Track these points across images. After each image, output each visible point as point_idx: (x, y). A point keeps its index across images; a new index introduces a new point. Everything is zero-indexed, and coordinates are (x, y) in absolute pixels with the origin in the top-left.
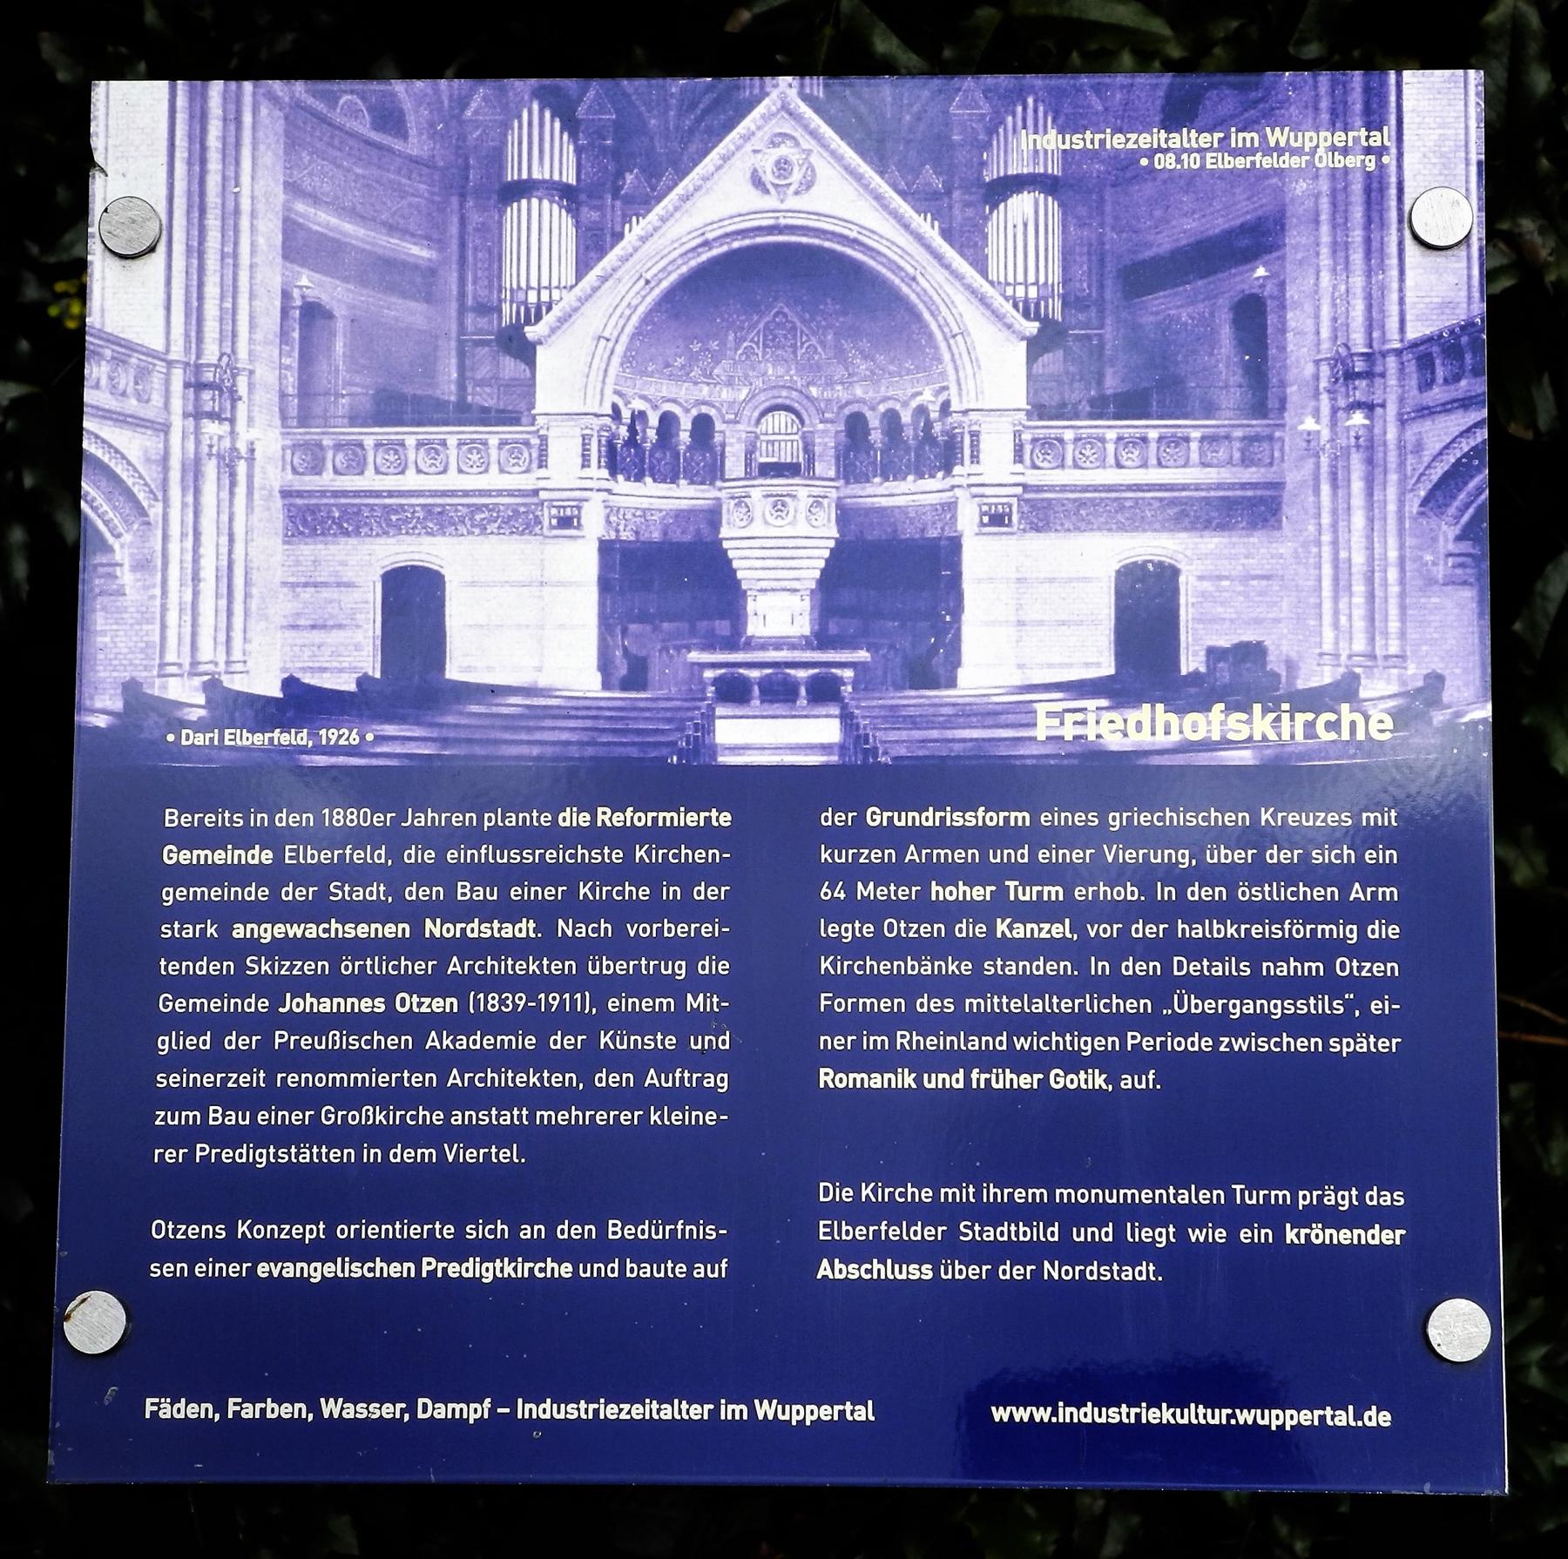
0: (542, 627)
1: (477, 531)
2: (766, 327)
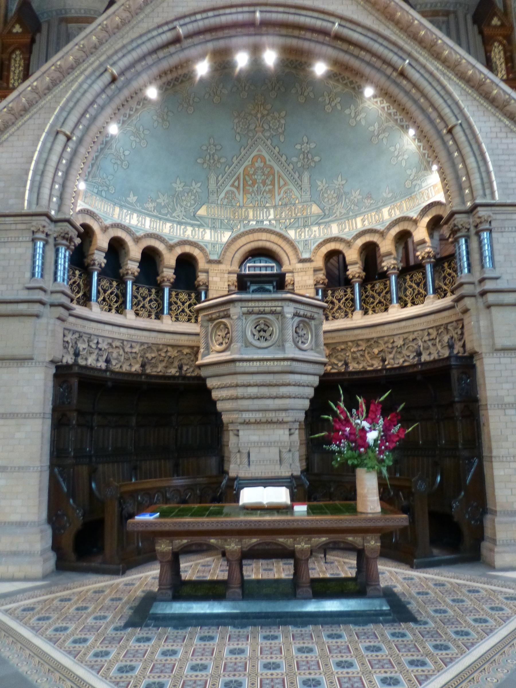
2: (246, 173)
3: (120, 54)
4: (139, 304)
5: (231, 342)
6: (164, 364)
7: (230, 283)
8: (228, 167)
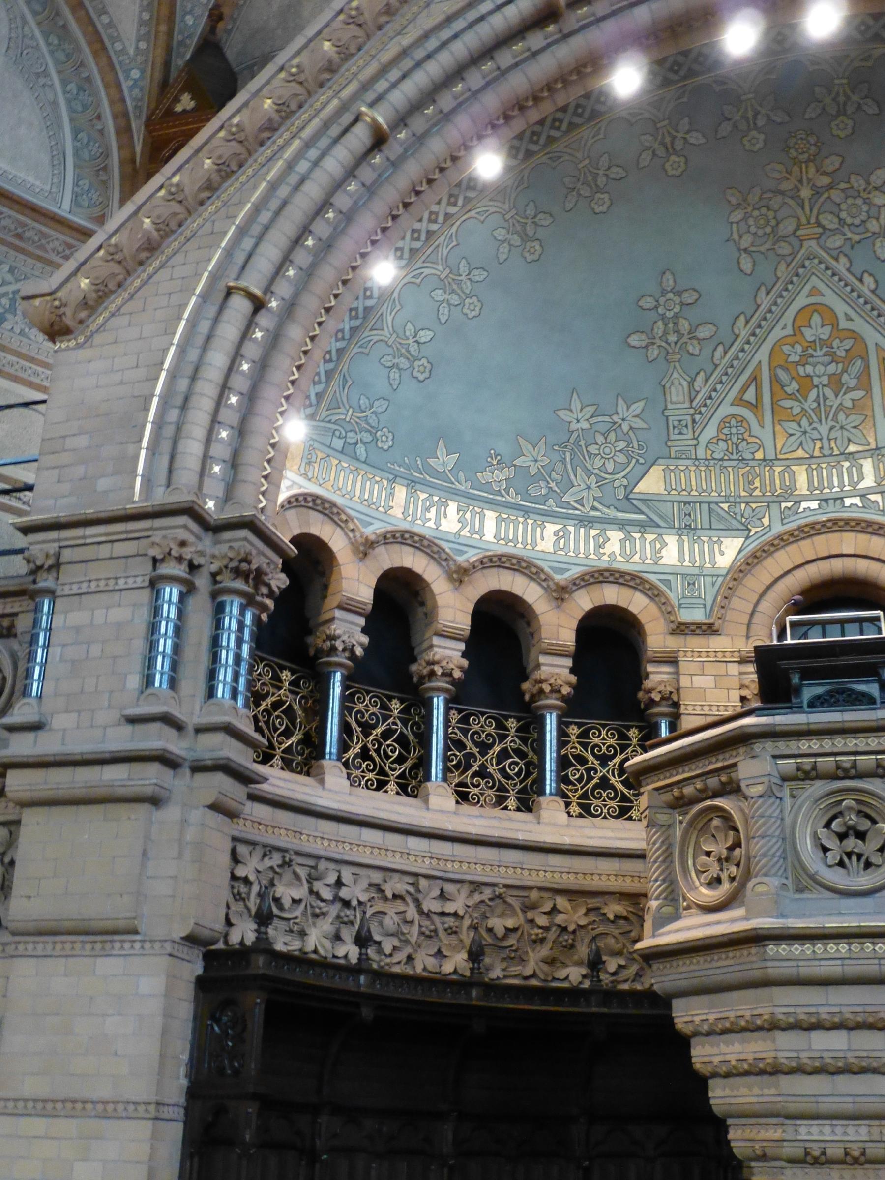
3: (394, 74)
4: (468, 766)
5: (747, 875)
6: (544, 951)
7: (745, 693)
8: (720, 349)
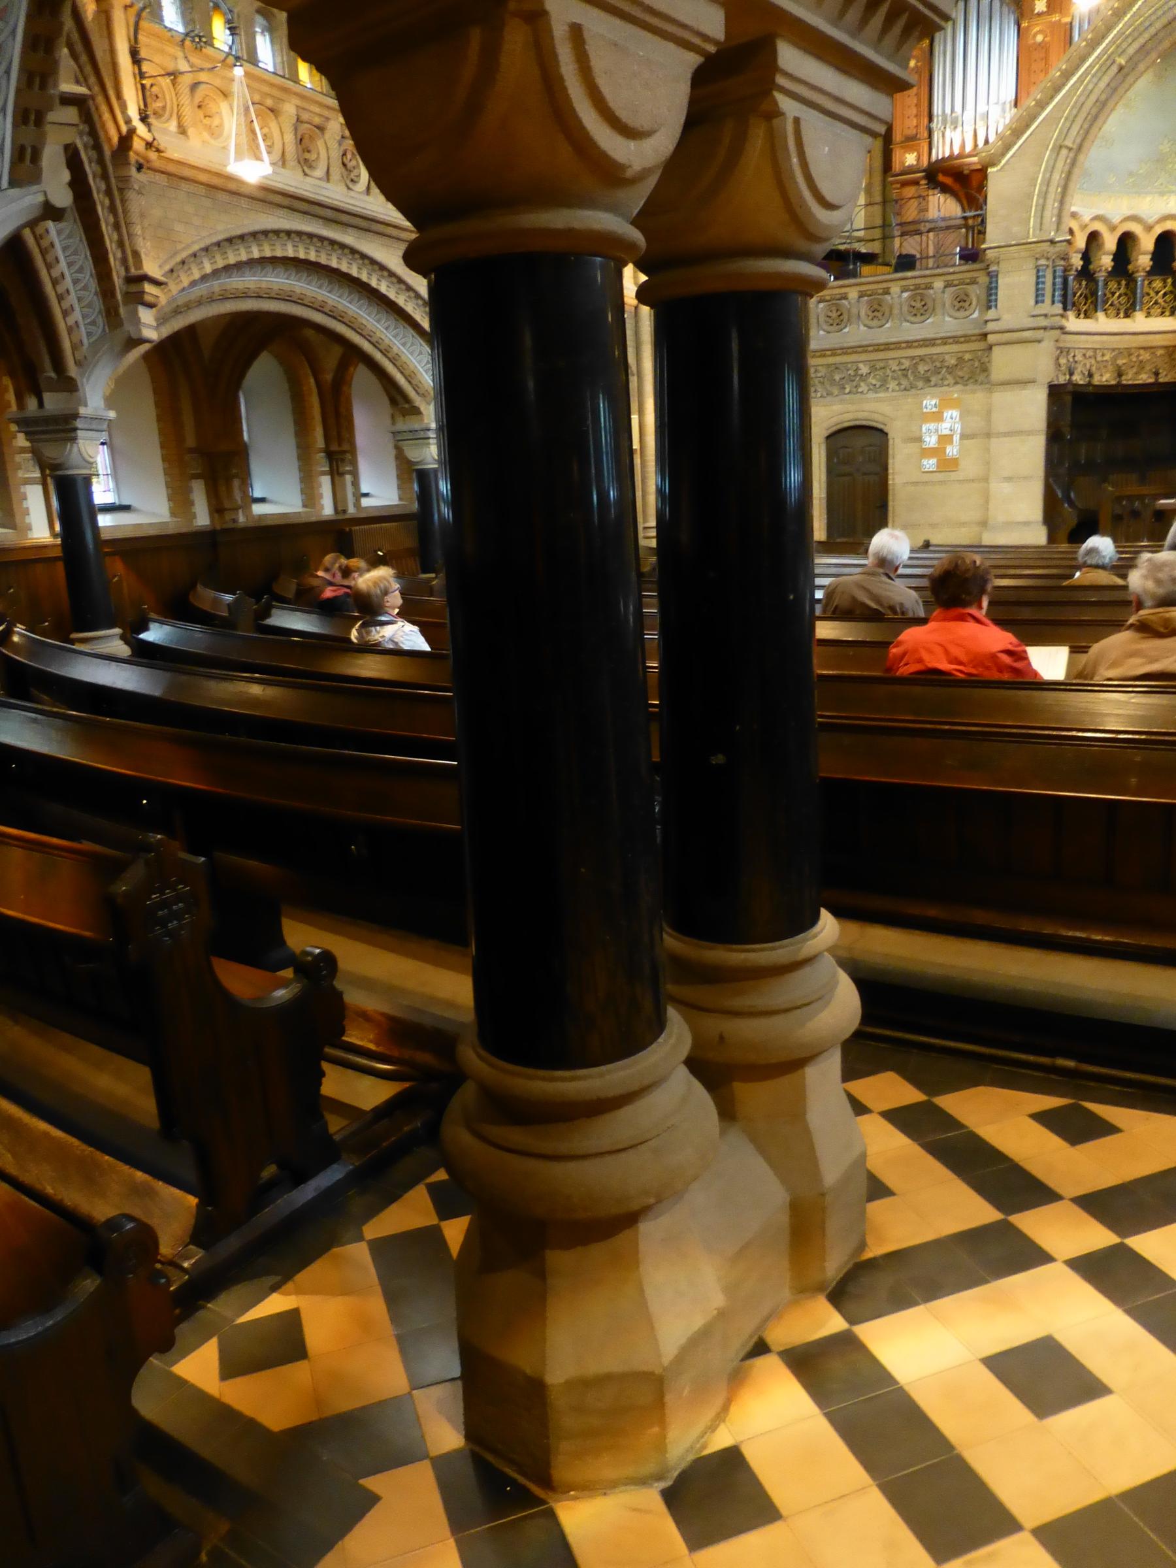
0: (986, 479)
1: (920, 384)
3: (1130, 40)
